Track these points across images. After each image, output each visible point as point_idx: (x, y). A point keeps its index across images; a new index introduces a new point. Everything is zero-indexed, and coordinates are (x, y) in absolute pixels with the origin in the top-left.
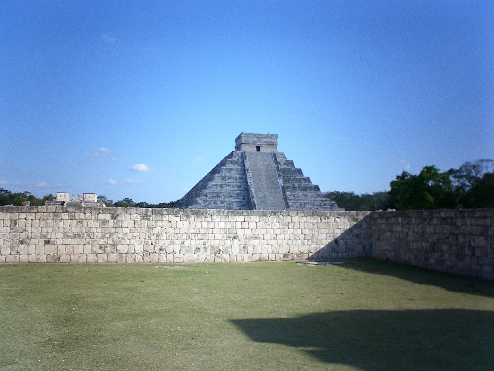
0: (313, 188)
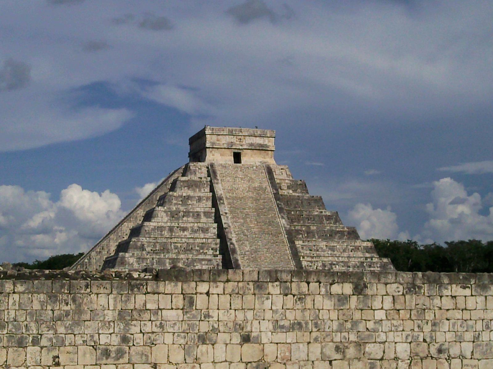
0: (346, 233)
